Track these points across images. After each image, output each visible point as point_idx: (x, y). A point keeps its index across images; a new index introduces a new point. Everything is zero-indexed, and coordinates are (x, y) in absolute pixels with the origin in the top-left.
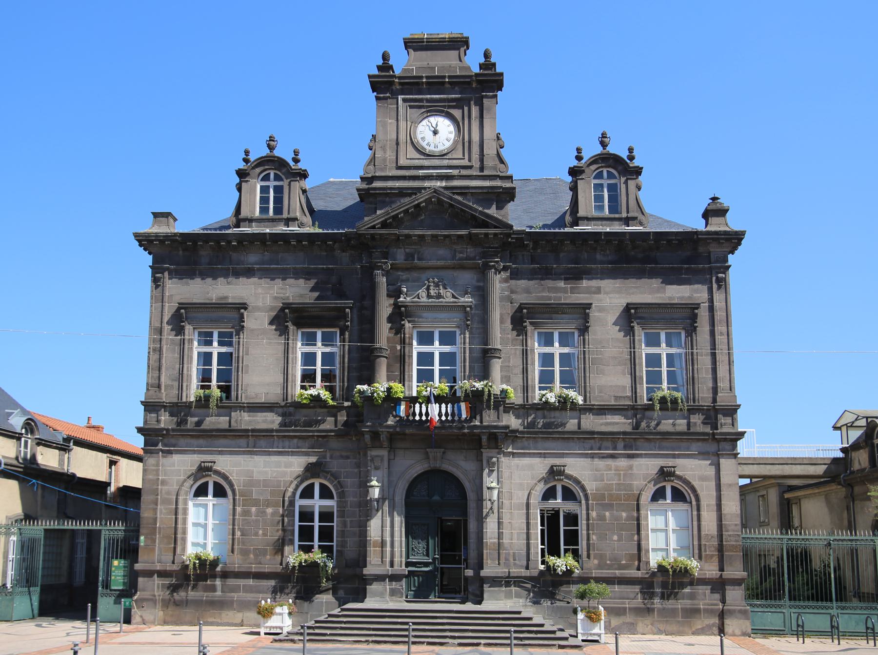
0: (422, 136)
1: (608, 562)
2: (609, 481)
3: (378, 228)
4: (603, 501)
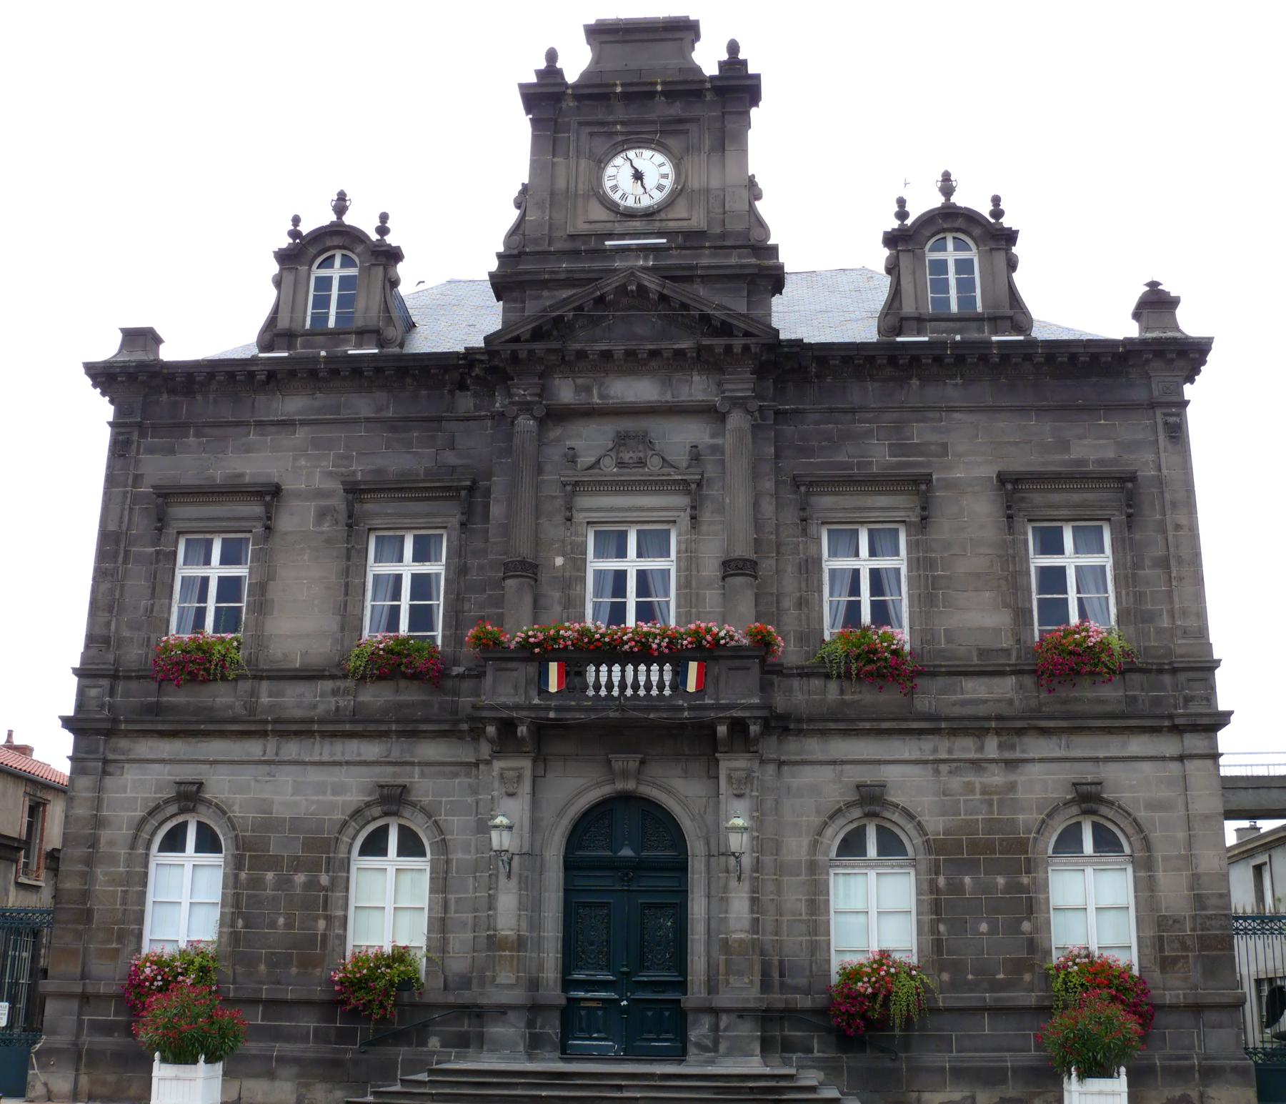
0: (613, 183)
1: (970, 977)
2: (971, 814)
3: (526, 341)
4: (958, 854)
